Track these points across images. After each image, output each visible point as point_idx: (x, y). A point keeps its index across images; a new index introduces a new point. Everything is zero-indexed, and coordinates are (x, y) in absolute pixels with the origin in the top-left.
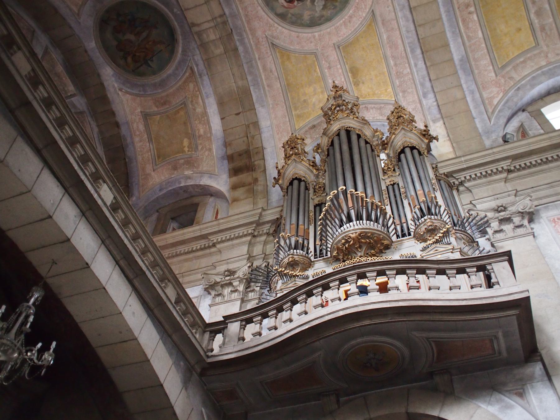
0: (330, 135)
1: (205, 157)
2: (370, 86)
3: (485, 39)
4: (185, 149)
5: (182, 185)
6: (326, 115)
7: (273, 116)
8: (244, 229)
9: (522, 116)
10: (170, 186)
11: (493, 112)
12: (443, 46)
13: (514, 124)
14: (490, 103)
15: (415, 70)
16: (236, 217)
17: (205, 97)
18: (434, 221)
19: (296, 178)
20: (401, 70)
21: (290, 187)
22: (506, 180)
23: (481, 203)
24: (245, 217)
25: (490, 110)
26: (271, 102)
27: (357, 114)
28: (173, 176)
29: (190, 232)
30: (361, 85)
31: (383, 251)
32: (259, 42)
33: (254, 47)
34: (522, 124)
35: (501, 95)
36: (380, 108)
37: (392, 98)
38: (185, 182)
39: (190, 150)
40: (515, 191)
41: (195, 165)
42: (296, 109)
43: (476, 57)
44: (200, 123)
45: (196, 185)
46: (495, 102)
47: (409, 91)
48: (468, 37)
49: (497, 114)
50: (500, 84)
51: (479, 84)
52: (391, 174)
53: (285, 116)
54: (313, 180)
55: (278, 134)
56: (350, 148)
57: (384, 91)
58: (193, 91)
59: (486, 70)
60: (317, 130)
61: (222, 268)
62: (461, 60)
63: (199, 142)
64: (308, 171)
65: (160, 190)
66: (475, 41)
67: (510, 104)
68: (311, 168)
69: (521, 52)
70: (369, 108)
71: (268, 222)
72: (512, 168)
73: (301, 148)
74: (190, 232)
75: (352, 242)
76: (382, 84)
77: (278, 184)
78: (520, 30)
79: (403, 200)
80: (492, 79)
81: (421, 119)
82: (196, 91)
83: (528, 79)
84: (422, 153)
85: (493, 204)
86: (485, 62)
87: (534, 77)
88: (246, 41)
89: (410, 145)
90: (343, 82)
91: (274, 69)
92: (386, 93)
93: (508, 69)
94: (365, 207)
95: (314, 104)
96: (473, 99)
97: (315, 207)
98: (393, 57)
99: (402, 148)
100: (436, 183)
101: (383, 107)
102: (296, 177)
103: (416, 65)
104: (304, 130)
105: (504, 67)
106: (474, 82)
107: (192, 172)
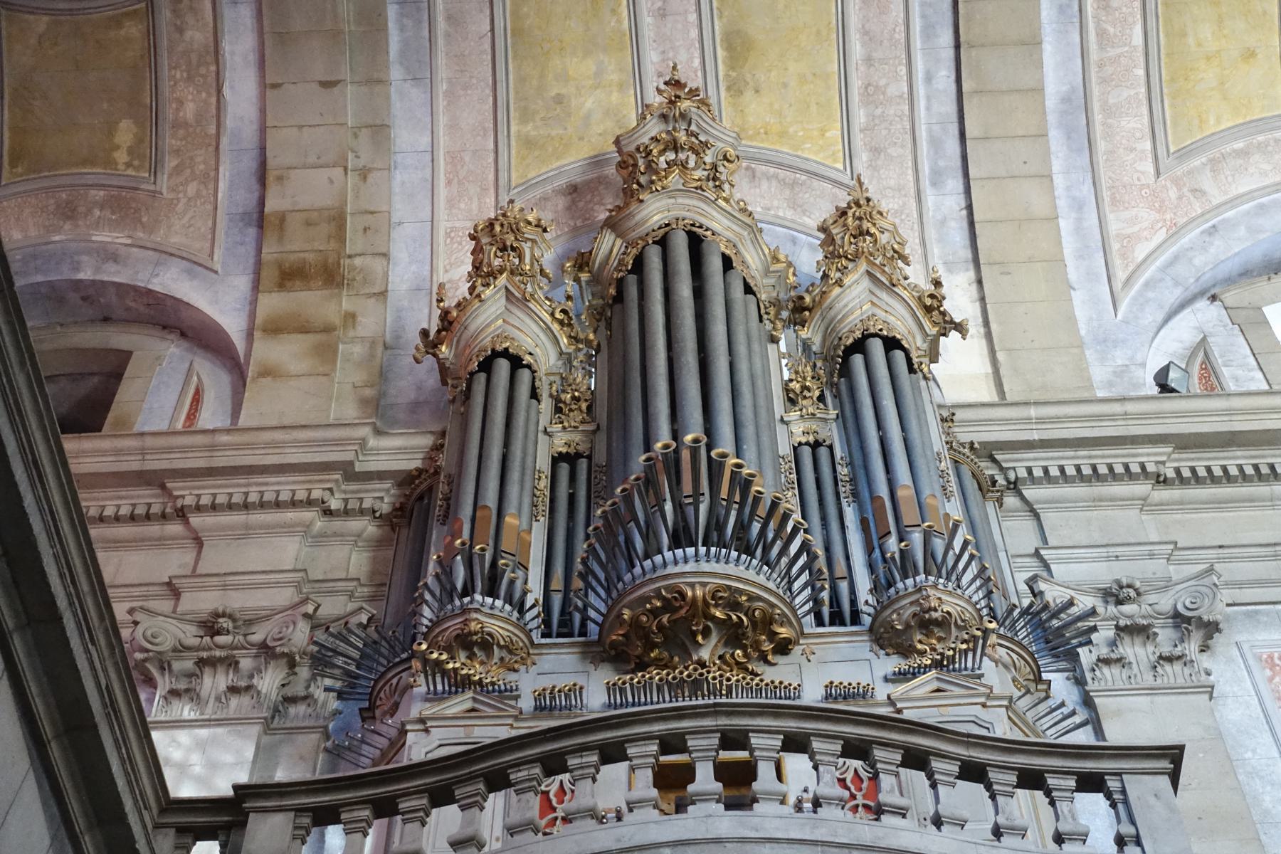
0: (633, 235)
1: (184, 201)
2: (776, 106)
3: (1147, 55)
4: (116, 155)
5: (81, 276)
6: (626, 164)
8: (294, 482)
9: (1205, 314)
10: (38, 270)
11: (1128, 282)
12: (1023, 43)
13: (1181, 334)
14: (1124, 256)
15: (921, 90)
16: (279, 436)
18: (944, 597)
19: (505, 354)
20: (882, 82)
21: (482, 376)
22: (1144, 504)
23: (1069, 561)
24: (309, 443)
25: (1120, 275)
27: (726, 186)
28: (57, 238)
29: (104, 453)
30: (749, 94)
31: (770, 657)
34: (1204, 339)
35: (1161, 235)
36: (794, 184)
37: (835, 161)
38: (97, 270)
39: (136, 163)
40: (1171, 547)
41: (145, 219)
42: (526, 116)
43: (1111, 101)
44: (190, 79)
45: (135, 288)
46: (1140, 253)
47: (893, 151)
48: (1101, 34)
49: (1140, 293)
50: (1163, 201)
51: (1104, 183)
52: (811, 410)
54: (555, 370)
55: (449, 183)
56: (699, 294)
57: (816, 133)
59: (1132, 150)
60: (581, 204)
61: (202, 601)
62: (1066, 100)
64: (542, 336)
66: (1119, 51)
67: (1181, 269)
68: (555, 327)
69: (1241, 121)
70: (758, 174)
71: (380, 476)
72: (1171, 474)
73: (533, 255)
74: (104, 453)
75: (683, 612)
76: (814, 108)
77: (435, 355)
78: (1250, 55)
79: (844, 502)
80: (1144, 182)
83: (1246, 207)
84: (916, 366)
85: (1105, 573)
86: (1132, 125)
87: (1262, 207)
89: (885, 333)
90: (695, 72)
92: (821, 142)
93: (1197, 162)
94: (736, 506)
95: (588, 117)
96: (1078, 230)
97: (557, 460)
98: (866, 33)
99: (858, 334)
100: (950, 472)
101: (804, 181)
102: (506, 349)
103: (929, 78)
104: (538, 192)
105: (1184, 154)
106: (1090, 175)
107: (129, 241)
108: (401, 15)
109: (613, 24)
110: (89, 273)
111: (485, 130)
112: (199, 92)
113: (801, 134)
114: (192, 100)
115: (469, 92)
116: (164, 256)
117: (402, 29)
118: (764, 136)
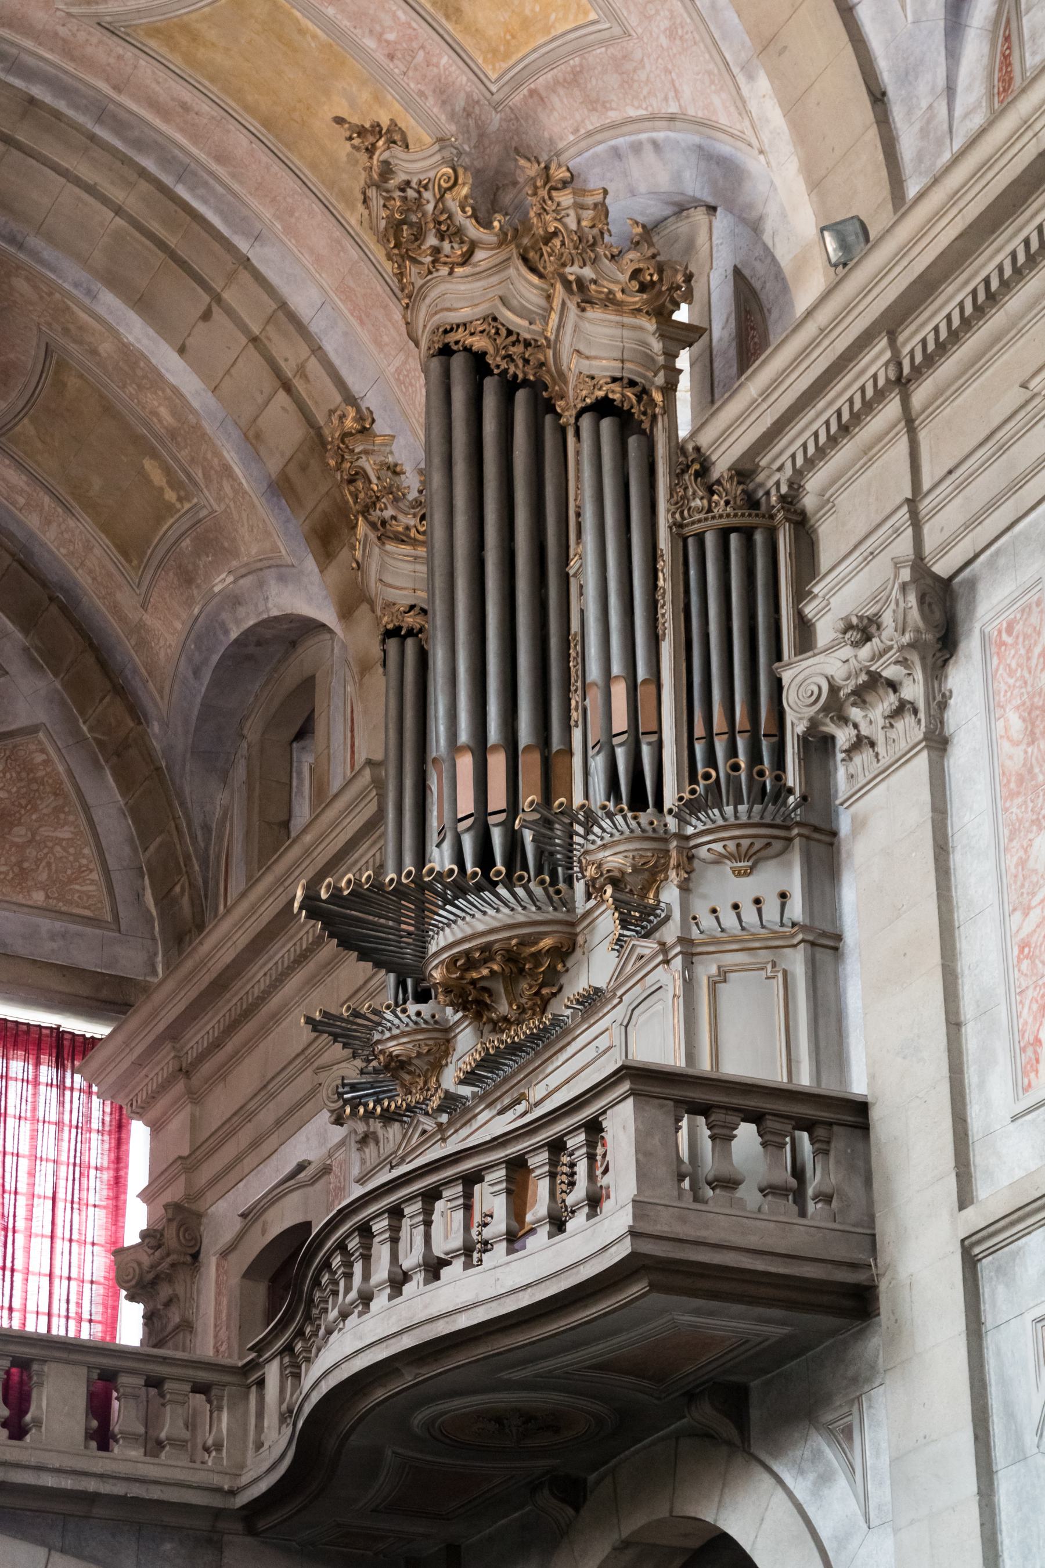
1: (232, 504)
5: (234, 635)
7: (307, 260)
17: (87, 301)
26: (267, 214)
28: (196, 611)
32: (64, 40)
33: (70, 67)
37: (586, 13)
38: (238, 622)
39: (182, 493)
41: (226, 544)
53: (338, 242)
58: (41, 298)
63: (183, 455)
65: (197, 673)
81: (709, 73)
82: (50, 294)
88: (30, 61)
90: (409, 24)
91: (186, 95)
101: (581, 65)
108: (192, 189)
109: (313, 45)
110: (234, 629)
111: (338, 242)
112: (156, 393)
113: (537, 9)
114: (160, 405)
115: (296, 214)
116: (260, 573)
117: (205, 201)
118: (513, 42)
